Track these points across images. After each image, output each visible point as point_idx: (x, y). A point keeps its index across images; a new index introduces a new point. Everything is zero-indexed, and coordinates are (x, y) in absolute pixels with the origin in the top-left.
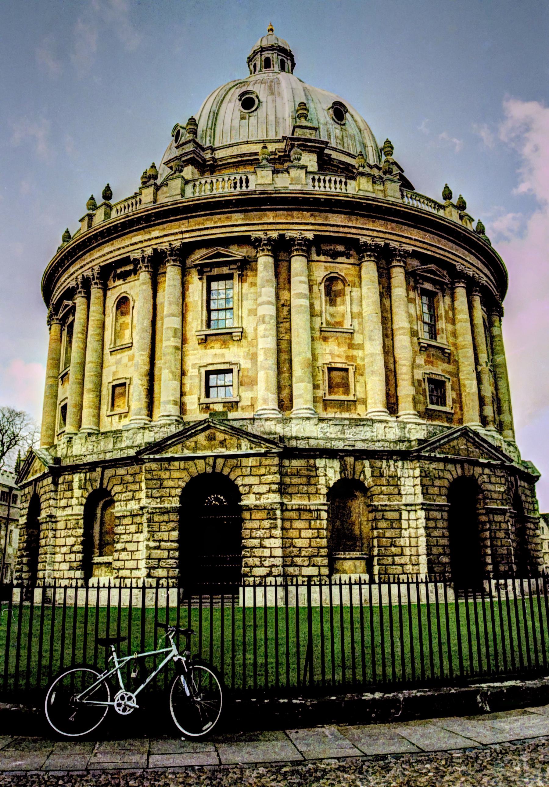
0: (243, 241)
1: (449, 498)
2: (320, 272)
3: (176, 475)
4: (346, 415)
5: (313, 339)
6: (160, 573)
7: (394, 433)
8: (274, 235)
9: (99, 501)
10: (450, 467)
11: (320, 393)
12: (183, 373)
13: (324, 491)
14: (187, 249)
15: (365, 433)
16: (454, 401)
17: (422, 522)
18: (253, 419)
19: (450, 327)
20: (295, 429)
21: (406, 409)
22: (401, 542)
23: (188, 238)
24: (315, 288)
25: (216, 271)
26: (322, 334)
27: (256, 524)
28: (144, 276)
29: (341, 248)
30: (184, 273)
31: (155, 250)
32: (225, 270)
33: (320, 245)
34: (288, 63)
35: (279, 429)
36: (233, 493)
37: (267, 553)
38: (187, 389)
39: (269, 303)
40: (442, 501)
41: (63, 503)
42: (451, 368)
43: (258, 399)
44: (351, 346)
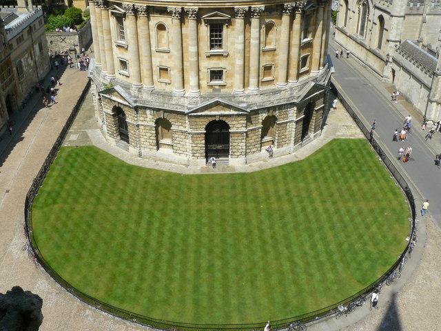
3: (203, 120)
6: (197, 155)
7: (287, 95)
12: (199, 70)
13: (261, 121)
15: (278, 96)
17: (294, 126)
20: (251, 100)
26: (262, 52)
27: (236, 138)
28: (176, 22)
30: (198, 21)
31: (183, 8)
36: (227, 127)
37: (240, 147)
38: (201, 77)
39: (240, 44)
41: (142, 118)
43: (233, 85)
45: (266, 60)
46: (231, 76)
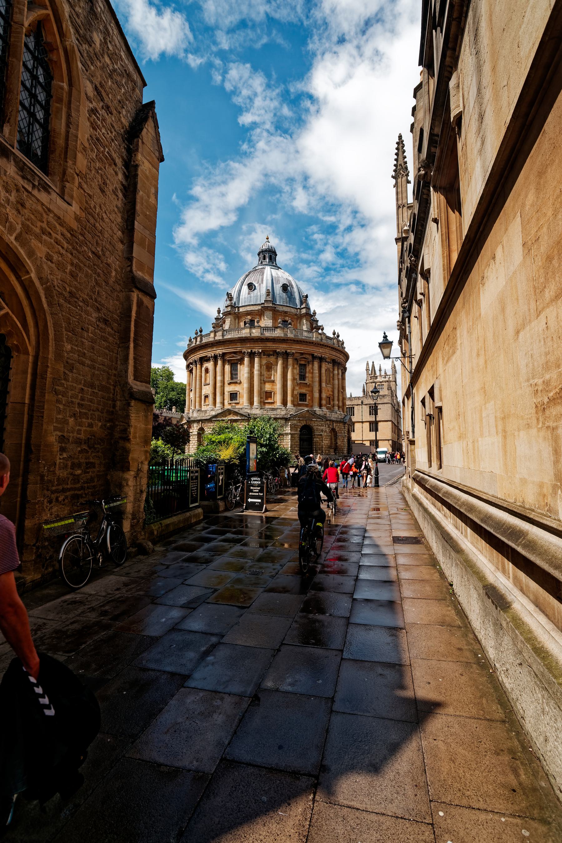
0: (241, 352)
1: (300, 431)
2: (264, 362)
4: (270, 407)
5: (261, 383)
8: (249, 351)
9: (201, 430)
10: (302, 422)
11: (262, 400)
14: (224, 354)
15: (275, 412)
16: (309, 400)
18: (242, 409)
19: (310, 375)
21: (289, 404)
22: (284, 444)
23: (224, 351)
24: (262, 367)
25: (233, 362)
26: (262, 382)
29: (271, 353)
32: (236, 362)
33: (265, 353)
34: (273, 256)
35: (249, 411)
40: (298, 432)
42: (309, 389)
44: (273, 385)
45: (268, 387)
46: (243, 397)
